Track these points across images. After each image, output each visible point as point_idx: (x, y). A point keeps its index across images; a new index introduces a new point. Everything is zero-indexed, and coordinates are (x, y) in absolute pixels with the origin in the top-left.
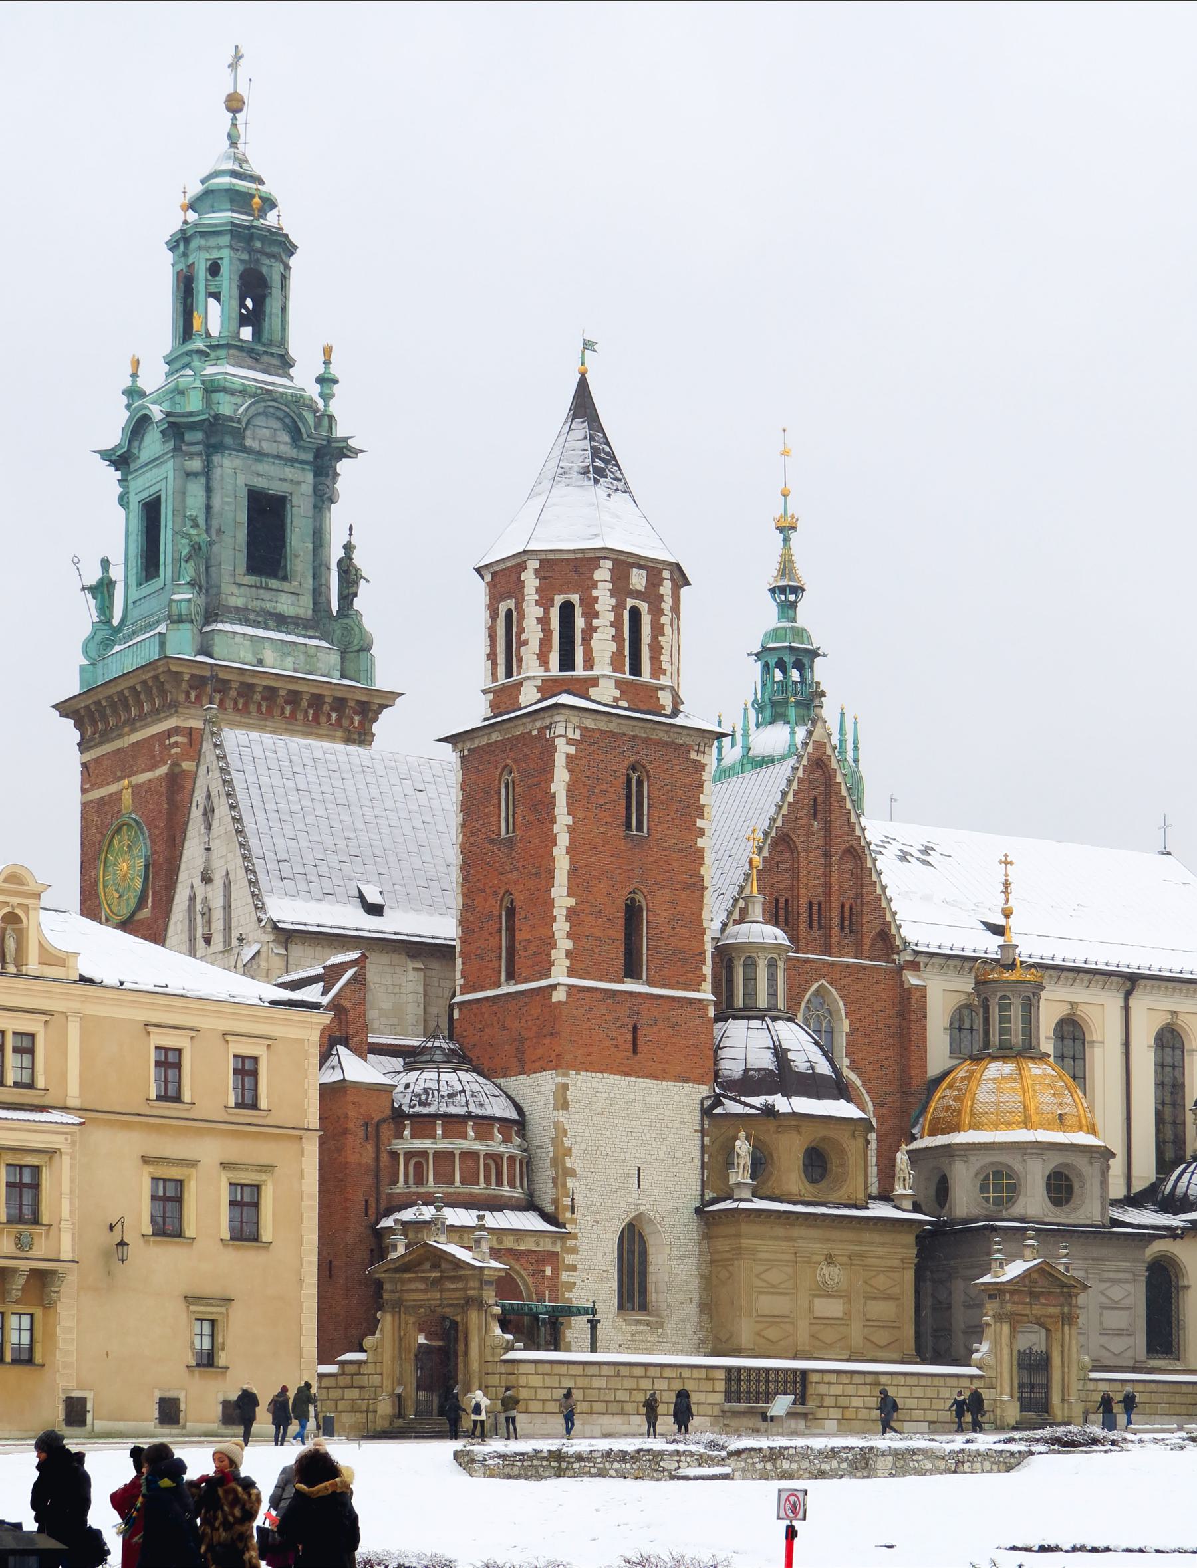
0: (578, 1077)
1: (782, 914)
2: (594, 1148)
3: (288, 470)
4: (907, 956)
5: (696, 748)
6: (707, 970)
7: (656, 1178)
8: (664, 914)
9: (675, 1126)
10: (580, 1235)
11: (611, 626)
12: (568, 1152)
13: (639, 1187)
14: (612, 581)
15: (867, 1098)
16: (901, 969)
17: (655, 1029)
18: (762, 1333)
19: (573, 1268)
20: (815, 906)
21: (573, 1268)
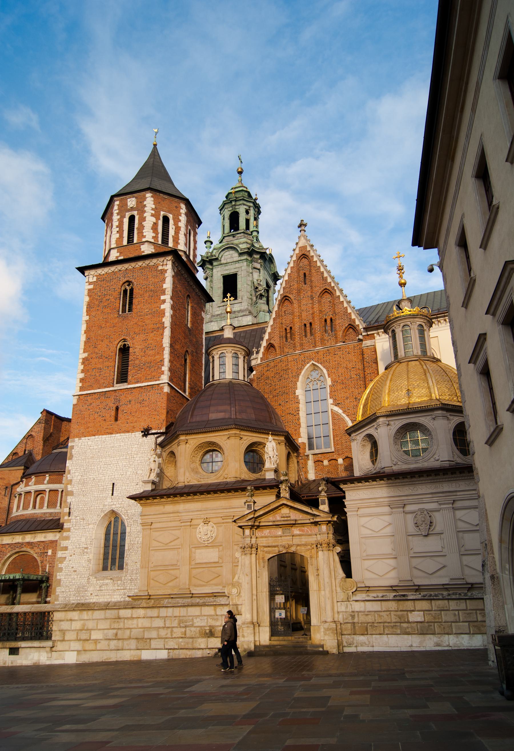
0: (81, 441)
1: (289, 335)
2: (85, 477)
3: (237, 265)
4: (363, 334)
5: (162, 264)
6: (165, 368)
7: (124, 488)
8: (139, 347)
9: (138, 456)
10: (72, 528)
12: (70, 482)
13: (112, 494)
15: (347, 419)
17: (129, 406)
18: (155, 579)
19: (66, 549)
21: (66, 549)
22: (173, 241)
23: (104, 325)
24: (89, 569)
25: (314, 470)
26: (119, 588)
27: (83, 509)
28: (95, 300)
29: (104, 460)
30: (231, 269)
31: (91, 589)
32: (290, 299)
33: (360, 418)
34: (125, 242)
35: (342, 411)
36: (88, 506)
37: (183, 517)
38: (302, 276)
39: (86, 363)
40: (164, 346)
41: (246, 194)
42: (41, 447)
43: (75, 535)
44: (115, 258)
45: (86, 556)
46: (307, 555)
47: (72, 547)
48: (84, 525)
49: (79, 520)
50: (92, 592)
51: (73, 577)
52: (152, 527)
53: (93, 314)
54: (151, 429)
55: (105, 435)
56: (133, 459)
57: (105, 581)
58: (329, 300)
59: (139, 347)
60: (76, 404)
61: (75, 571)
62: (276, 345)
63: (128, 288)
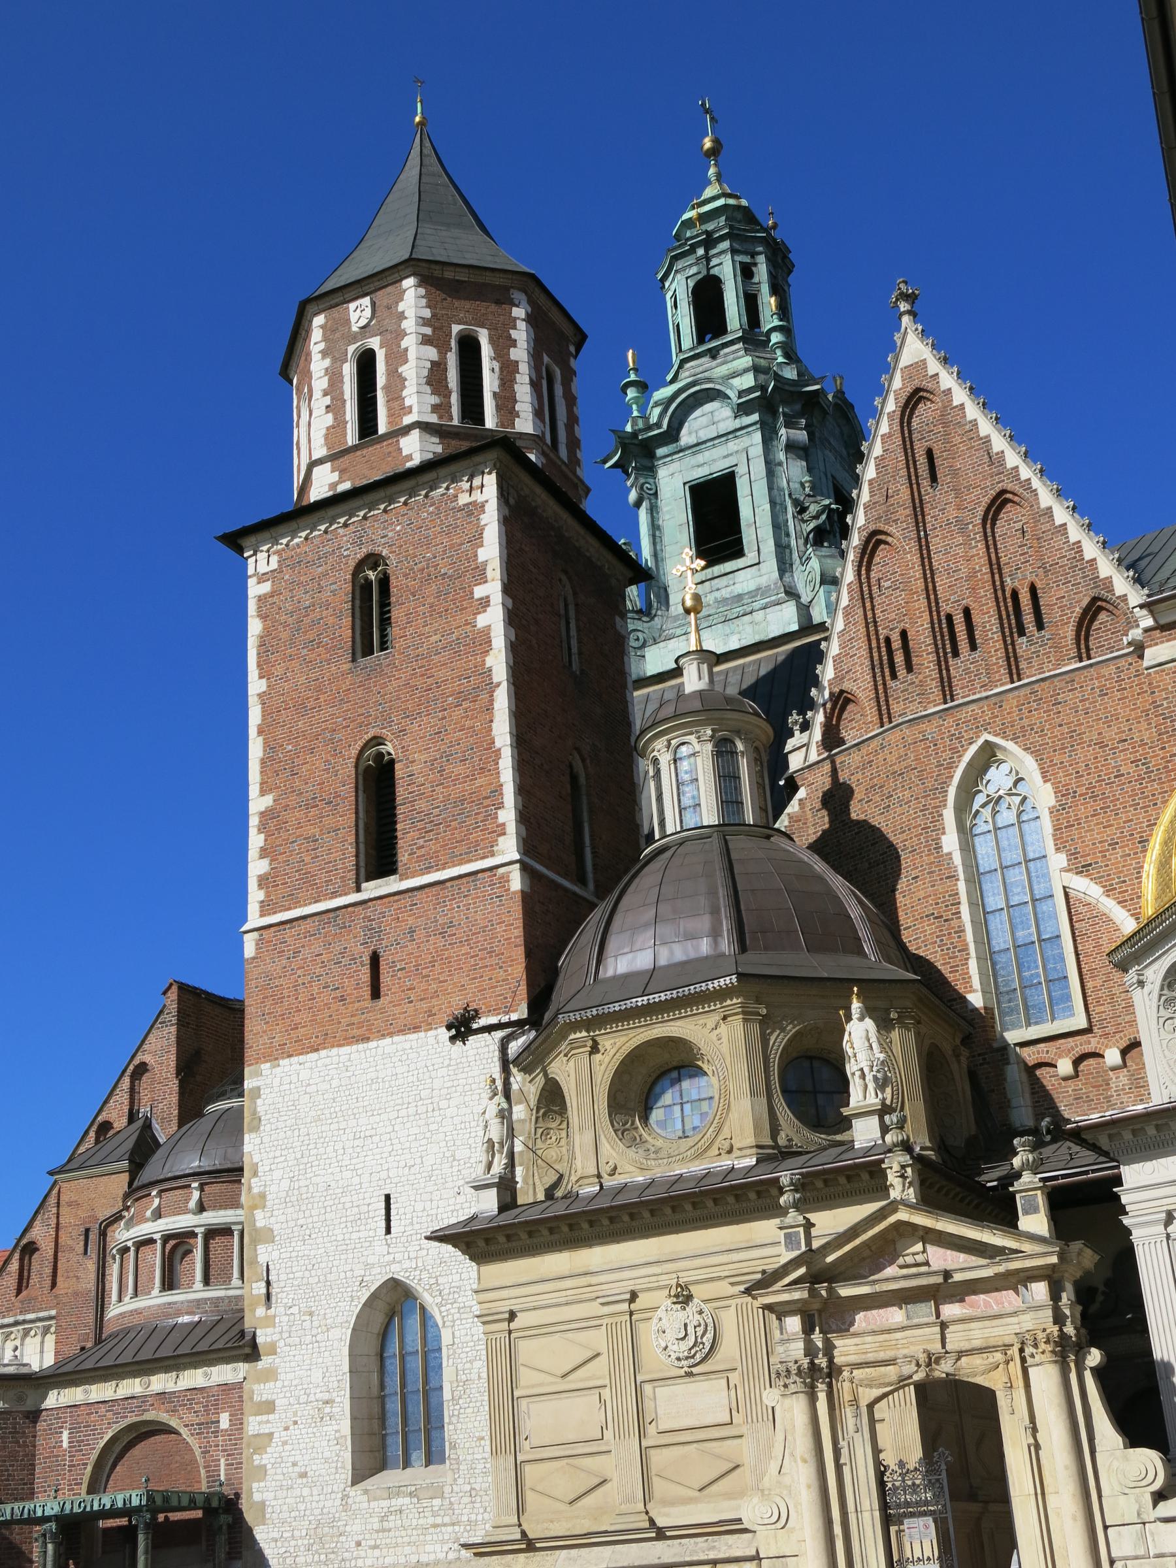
0: (278, 1070)
1: (899, 658)
2: (302, 1183)
6: (508, 815)
7: (419, 1206)
8: (423, 757)
9: (453, 1103)
10: (281, 1343)
11: (325, 394)
13: (388, 1231)
14: (325, 338)
16: (1139, 649)
17: (411, 947)
19: (269, 1407)
20: (959, 619)
21: (269, 1407)
22: (498, 408)
23: (312, 703)
24: (343, 1468)
25: (1027, 1095)
26: (439, 1520)
27: (305, 1281)
28: (281, 628)
29: (353, 1123)
30: (714, 460)
31: (355, 1528)
32: (889, 539)
33: (1149, 910)
34: (351, 436)
35: (1102, 890)
36: (319, 1272)
37: (604, 1287)
38: (922, 460)
39: (272, 825)
40: (498, 744)
41: (739, 216)
42: (175, 1099)
43: (293, 1364)
44: (326, 488)
45: (330, 1428)
46: (994, 1381)
47: (285, 1401)
48: (314, 1332)
49: (297, 1316)
50: (360, 1538)
51: (297, 1492)
52: (513, 1325)
53: (279, 670)
54: (477, 1014)
55: (349, 1044)
56: (436, 1113)
57: (394, 1502)
58: (1018, 526)
59: (423, 757)
60: (254, 958)
61: (303, 1475)
62: (861, 695)
63: (372, 575)
